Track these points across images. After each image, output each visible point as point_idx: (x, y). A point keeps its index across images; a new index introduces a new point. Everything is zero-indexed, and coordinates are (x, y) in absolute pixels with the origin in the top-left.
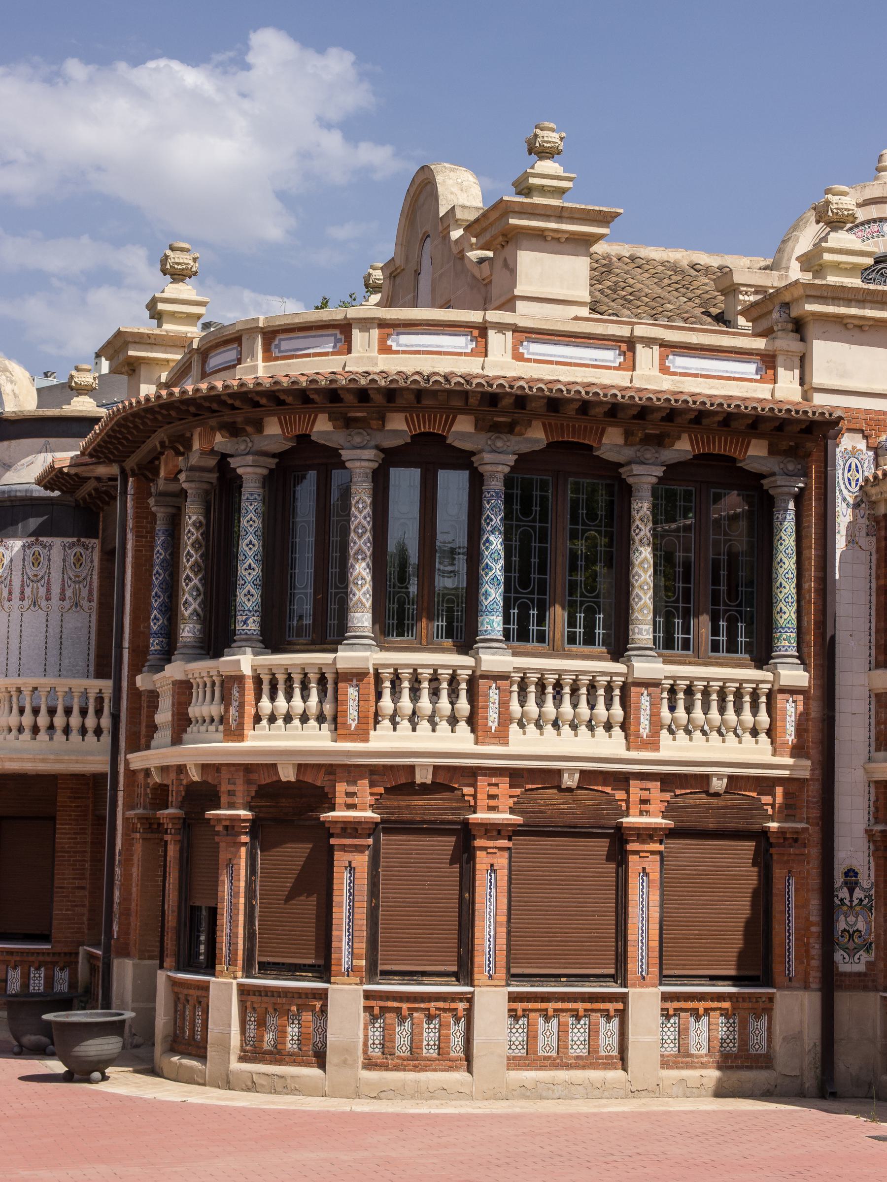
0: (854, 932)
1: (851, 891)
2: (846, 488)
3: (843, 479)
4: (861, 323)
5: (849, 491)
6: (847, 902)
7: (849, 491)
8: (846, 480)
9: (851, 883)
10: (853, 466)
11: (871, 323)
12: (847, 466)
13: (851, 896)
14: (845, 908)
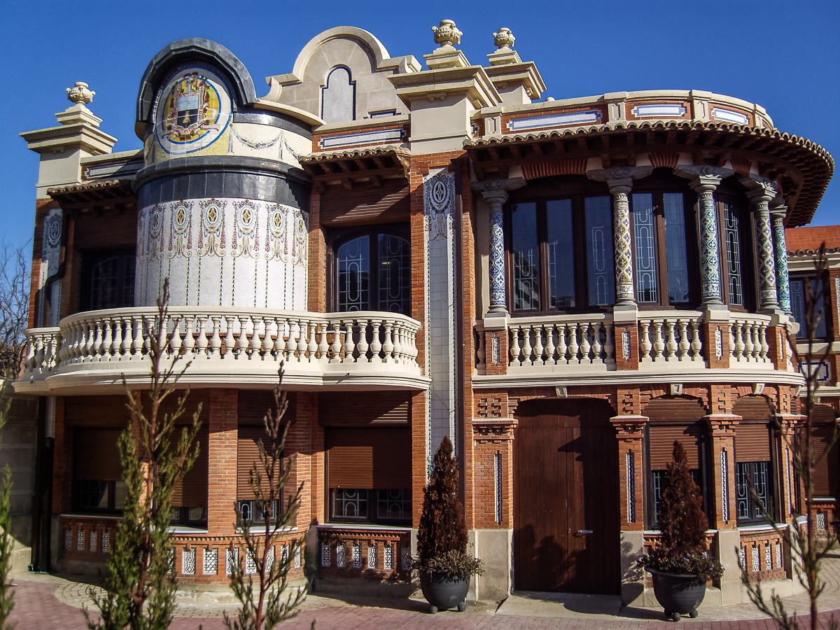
2: (435, 201)
3: (433, 196)
5: (437, 203)
7: (437, 203)
8: (435, 195)
10: (439, 187)
11: (445, 94)
12: (435, 187)
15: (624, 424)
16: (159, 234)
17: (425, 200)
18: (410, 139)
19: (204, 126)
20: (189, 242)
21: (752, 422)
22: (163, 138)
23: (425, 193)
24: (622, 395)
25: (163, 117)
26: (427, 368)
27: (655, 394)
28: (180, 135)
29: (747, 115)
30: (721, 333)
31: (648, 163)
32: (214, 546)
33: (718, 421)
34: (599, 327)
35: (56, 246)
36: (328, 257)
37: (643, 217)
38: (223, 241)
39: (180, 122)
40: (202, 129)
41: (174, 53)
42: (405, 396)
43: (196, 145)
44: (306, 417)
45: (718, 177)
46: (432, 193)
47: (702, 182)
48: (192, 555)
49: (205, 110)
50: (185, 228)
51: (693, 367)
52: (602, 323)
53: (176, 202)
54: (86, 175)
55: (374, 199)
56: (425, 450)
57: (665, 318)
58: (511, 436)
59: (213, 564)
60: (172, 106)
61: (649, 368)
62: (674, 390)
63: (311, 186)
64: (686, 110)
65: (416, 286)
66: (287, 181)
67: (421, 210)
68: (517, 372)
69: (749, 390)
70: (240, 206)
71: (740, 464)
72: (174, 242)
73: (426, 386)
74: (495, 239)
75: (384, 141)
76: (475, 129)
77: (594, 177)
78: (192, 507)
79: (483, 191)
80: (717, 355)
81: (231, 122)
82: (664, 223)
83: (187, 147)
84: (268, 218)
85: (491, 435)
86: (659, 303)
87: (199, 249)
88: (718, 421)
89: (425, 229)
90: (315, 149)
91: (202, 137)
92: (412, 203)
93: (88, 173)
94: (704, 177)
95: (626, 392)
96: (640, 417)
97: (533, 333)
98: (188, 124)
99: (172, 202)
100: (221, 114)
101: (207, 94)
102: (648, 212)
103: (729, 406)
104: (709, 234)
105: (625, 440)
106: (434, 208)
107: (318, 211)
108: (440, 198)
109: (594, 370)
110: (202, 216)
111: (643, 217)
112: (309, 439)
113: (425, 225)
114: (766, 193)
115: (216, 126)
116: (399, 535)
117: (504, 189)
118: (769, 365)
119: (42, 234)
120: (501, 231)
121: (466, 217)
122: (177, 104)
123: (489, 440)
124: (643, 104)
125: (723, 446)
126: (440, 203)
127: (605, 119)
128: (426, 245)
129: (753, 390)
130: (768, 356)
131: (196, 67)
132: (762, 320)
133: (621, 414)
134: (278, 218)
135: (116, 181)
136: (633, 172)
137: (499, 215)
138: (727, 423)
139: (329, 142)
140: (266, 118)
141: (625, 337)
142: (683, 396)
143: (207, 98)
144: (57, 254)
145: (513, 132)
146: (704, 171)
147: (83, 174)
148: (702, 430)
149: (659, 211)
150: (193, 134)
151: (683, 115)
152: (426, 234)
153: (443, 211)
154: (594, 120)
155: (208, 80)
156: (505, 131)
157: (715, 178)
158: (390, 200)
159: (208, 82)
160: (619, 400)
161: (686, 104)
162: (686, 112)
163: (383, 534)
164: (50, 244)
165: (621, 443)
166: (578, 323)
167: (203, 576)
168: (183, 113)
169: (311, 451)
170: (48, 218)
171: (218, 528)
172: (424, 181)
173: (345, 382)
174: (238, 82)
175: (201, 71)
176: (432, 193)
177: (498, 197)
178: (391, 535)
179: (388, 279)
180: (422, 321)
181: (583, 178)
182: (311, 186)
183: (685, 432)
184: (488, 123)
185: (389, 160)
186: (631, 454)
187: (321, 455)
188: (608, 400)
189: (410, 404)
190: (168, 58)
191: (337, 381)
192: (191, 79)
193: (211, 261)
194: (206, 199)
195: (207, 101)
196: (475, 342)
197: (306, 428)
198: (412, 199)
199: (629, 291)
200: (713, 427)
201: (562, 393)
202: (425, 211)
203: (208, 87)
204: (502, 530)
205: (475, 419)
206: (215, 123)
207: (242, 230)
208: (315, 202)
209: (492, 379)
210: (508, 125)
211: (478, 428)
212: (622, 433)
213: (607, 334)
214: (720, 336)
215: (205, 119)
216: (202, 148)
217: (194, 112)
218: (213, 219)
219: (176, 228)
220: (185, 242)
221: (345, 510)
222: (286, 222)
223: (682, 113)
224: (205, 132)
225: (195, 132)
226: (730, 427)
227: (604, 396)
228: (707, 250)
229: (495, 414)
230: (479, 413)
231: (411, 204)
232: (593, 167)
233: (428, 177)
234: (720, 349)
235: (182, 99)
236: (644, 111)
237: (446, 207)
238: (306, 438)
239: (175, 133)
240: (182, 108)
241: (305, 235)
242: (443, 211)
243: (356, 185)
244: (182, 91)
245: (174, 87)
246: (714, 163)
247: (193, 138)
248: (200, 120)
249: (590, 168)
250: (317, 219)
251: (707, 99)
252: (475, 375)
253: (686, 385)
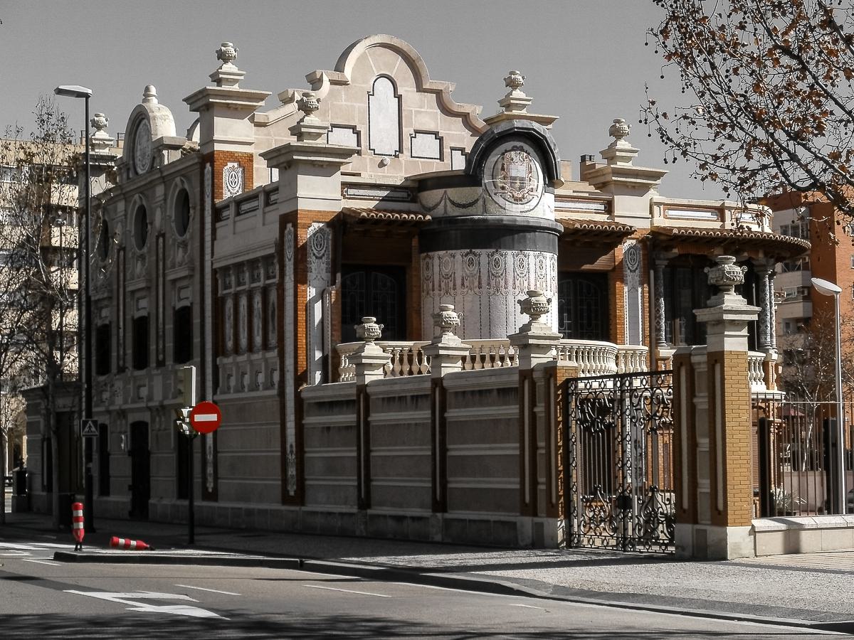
4: (634, 185)
16: (502, 274)
19: (531, 193)
22: (495, 194)
28: (513, 196)
35: (321, 258)
43: (527, 207)
60: (503, 169)
72: (517, 283)
83: (520, 207)
106: (629, 268)
144: (324, 266)
153: (635, 271)
164: (314, 254)
168: (515, 178)
179: (585, 314)
194: (537, 252)
195: (531, 172)
215: (531, 187)
216: (531, 210)
217: (522, 179)
219: (518, 272)
224: (531, 197)
235: (512, 166)
240: (513, 173)
244: (512, 159)
247: (524, 201)
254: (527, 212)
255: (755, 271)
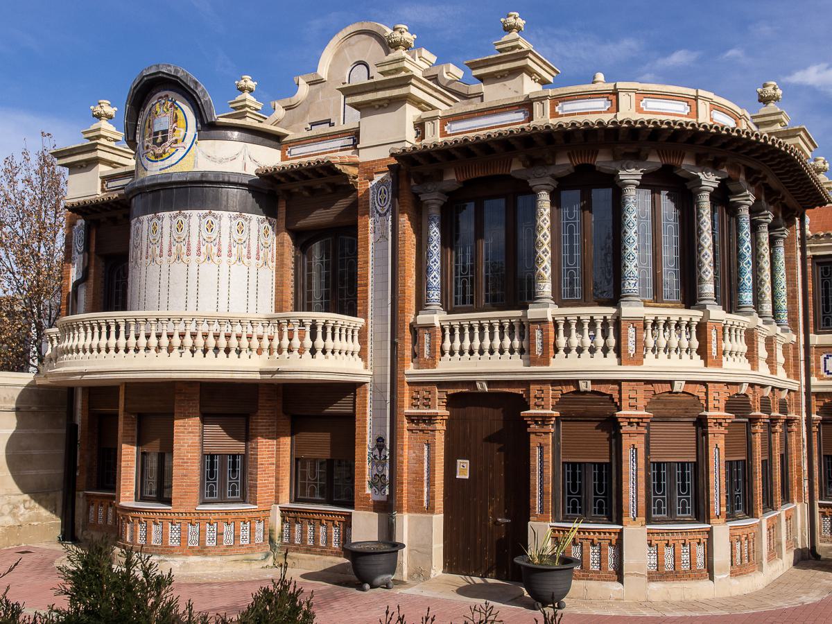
0: (382, 476)
1: (380, 451)
6: (378, 457)
9: (380, 446)
13: (380, 454)
14: (376, 461)
15: (534, 418)
17: (371, 204)
18: (358, 146)
19: (174, 146)
20: (161, 251)
21: (672, 419)
23: (371, 197)
24: (534, 389)
25: (144, 137)
26: (369, 362)
27: (566, 389)
28: (154, 153)
29: (688, 102)
30: (636, 330)
31: (567, 161)
32: (197, 521)
33: (627, 418)
34: (519, 323)
36: (296, 258)
37: (571, 214)
38: (188, 250)
39: (154, 142)
40: (171, 148)
41: (145, 78)
42: (349, 389)
43: (167, 163)
44: (270, 406)
45: (641, 172)
46: (377, 197)
47: (621, 178)
48: (160, 528)
49: (174, 130)
50: (157, 238)
51: (606, 365)
52: (520, 320)
53: (151, 215)
54: (105, 187)
55: (328, 205)
56: (365, 438)
57: (566, 316)
58: (440, 427)
59: (177, 536)
60: (149, 127)
61: (561, 365)
62: (583, 386)
63: (272, 194)
64: (612, 103)
65: (361, 285)
66: (250, 191)
67: (366, 213)
68: (448, 366)
69: (667, 387)
70: (204, 217)
71: (659, 465)
73: (367, 379)
74: (430, 240)
75: (339, 148)
76: (418, 133)
77: (518, 176)
78: (158, 487)
79: (421, 193)
80: (630, 352)
81: (196, 140)
82: (591, 218)
83: (160, 164)
84: (231, 227)
85: (422, 426)
86: (583, 300)
87: (169, 258)
88: (627, 418)
89: (369, 231)
90: (284, 158)
91: (171, 156)
92: (359, 208)
93: (107, 186)
94: (625, 172)
95: (538, 387)
96: (550, 412)
97: (462, 329)
98: (161, 143)
99: (149, 216)
100: (188, 133)
101: (176, 116)
102: (576, 210)
103: (642, 403)
104: (627, 230)
105: (535, 433)
106: (378, 212)
107: (284, 216)
108: (383, 202)
109: (510, 365)
110: (171, 227)
111: (571, 214)
112: (274, 425)
113: (370, 228)
114: (703, 183)
115: (183, 144)
116: (344, 515)
117: (439, 191)
118: (697, 361)
119: (71, 242)
120: (437, 231)
121: (404, 220)
122: (153, 124)
123: (420, 430)
124: (567, 101)
125: (632, 443)
126: (383, 207)
127: (530, 118)
128: (370, 247)
129: (672, 387)
130: (698, 352)
131: (166, 90)
132: (695, 315)
133: (534, 409)
134: (241, 225)
135: (116, 195)
136: (553, 171)
137: (435, 217)
138: (636, 420)
139: (296, 151)
140: (236, 134)
141: (538, 334)
142: (593, 392)
143: (176, 119)
145: (450, 135)
146: (624, 166)
147: (102, 186)
148: (611, 426)
149: (587, 207)
150: (164, 153)
151: (608, 109)
152: (371, 236)
153: (385, 214)
154: (521, 119)
155: (177, 102)
156: (444, 134)
157: (638, 172)
158: (342, 204)
159: (177, 104)
160: (532, 395)
161: (612, 97)
162: (612, 106)
163: (332, 515)
165: (532, 436)
166: (500, 319)
167: (168, 547)
168: (156, 134)
169: (276, 435)
170: (75, 227)
171: (180, 505)
172: (370, 185)
173: (278, 376)
174: (199, 103)
175: (172, 94)
176: (377, 197)
177: (433, 199)
178: (338, 515)
180: (366, 318)
181: (508, 178)
182: (272, 194)
183: (597, 428)
184: (428, 126)
185: (327, 170)
186: (541, 447)
187: (286, 441)
188: (522, 395)
189: (355, 395)
190: (142, 83)
191: (270, 376)
192: (163, 101)
193: (178, 268)
195: (176, 121)
196: (404, 338)
197: (269, 416)
198: (360, 203)
199: (546, 288)
200: (622, 424)
201: (482, 387)
202: (370, 215)
203: (177, 109)
204: (429, 515)
205: (407, 410)
206: (183, 141)
207: (205, 238)
208: (282, 210)
209: (426, 373)
210: (446, 127)
211: (411, 418)
212: (534, 427)
213: (523, 329)
214: (634, 333)
215: (174, 139)
217: (165, 132)
218: (180, 230)
220: (158, 252)
221: (308, 491)
222: (249, 230)
223: (607, 107)
224: (174, 150)
225: (166, 151)
226: (641, 424)
227: (519, 391)
228: (625, 247)
229: (426, 406)
230: (412, 405)
231: (356, 209)
232: (516, 167)
233: (374, 182)
234: (634, 346)
236: (569, 107)
237: (388, 211)
238: (269, 426)
239: (152, 152)
240: (156, 130)
241: (272, 239)
242: (385, 214)
243: (312, 191)
245: (150, 110)
246: (636, 157)
248: (170, 140)
249: (514, 168)
250: (283, 224)
251: (636, 91)
252: (410, 369)
253: (594, 382)
254: (167, 168)
255: (688, 188)
